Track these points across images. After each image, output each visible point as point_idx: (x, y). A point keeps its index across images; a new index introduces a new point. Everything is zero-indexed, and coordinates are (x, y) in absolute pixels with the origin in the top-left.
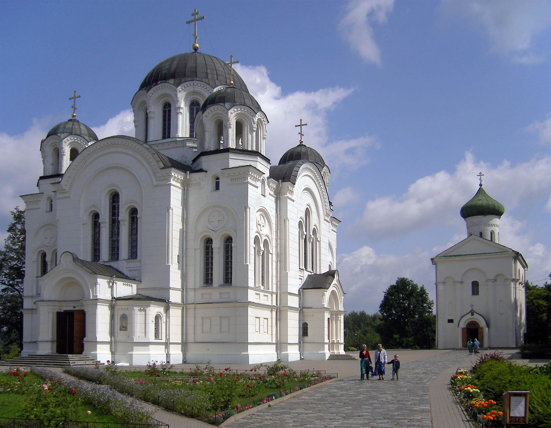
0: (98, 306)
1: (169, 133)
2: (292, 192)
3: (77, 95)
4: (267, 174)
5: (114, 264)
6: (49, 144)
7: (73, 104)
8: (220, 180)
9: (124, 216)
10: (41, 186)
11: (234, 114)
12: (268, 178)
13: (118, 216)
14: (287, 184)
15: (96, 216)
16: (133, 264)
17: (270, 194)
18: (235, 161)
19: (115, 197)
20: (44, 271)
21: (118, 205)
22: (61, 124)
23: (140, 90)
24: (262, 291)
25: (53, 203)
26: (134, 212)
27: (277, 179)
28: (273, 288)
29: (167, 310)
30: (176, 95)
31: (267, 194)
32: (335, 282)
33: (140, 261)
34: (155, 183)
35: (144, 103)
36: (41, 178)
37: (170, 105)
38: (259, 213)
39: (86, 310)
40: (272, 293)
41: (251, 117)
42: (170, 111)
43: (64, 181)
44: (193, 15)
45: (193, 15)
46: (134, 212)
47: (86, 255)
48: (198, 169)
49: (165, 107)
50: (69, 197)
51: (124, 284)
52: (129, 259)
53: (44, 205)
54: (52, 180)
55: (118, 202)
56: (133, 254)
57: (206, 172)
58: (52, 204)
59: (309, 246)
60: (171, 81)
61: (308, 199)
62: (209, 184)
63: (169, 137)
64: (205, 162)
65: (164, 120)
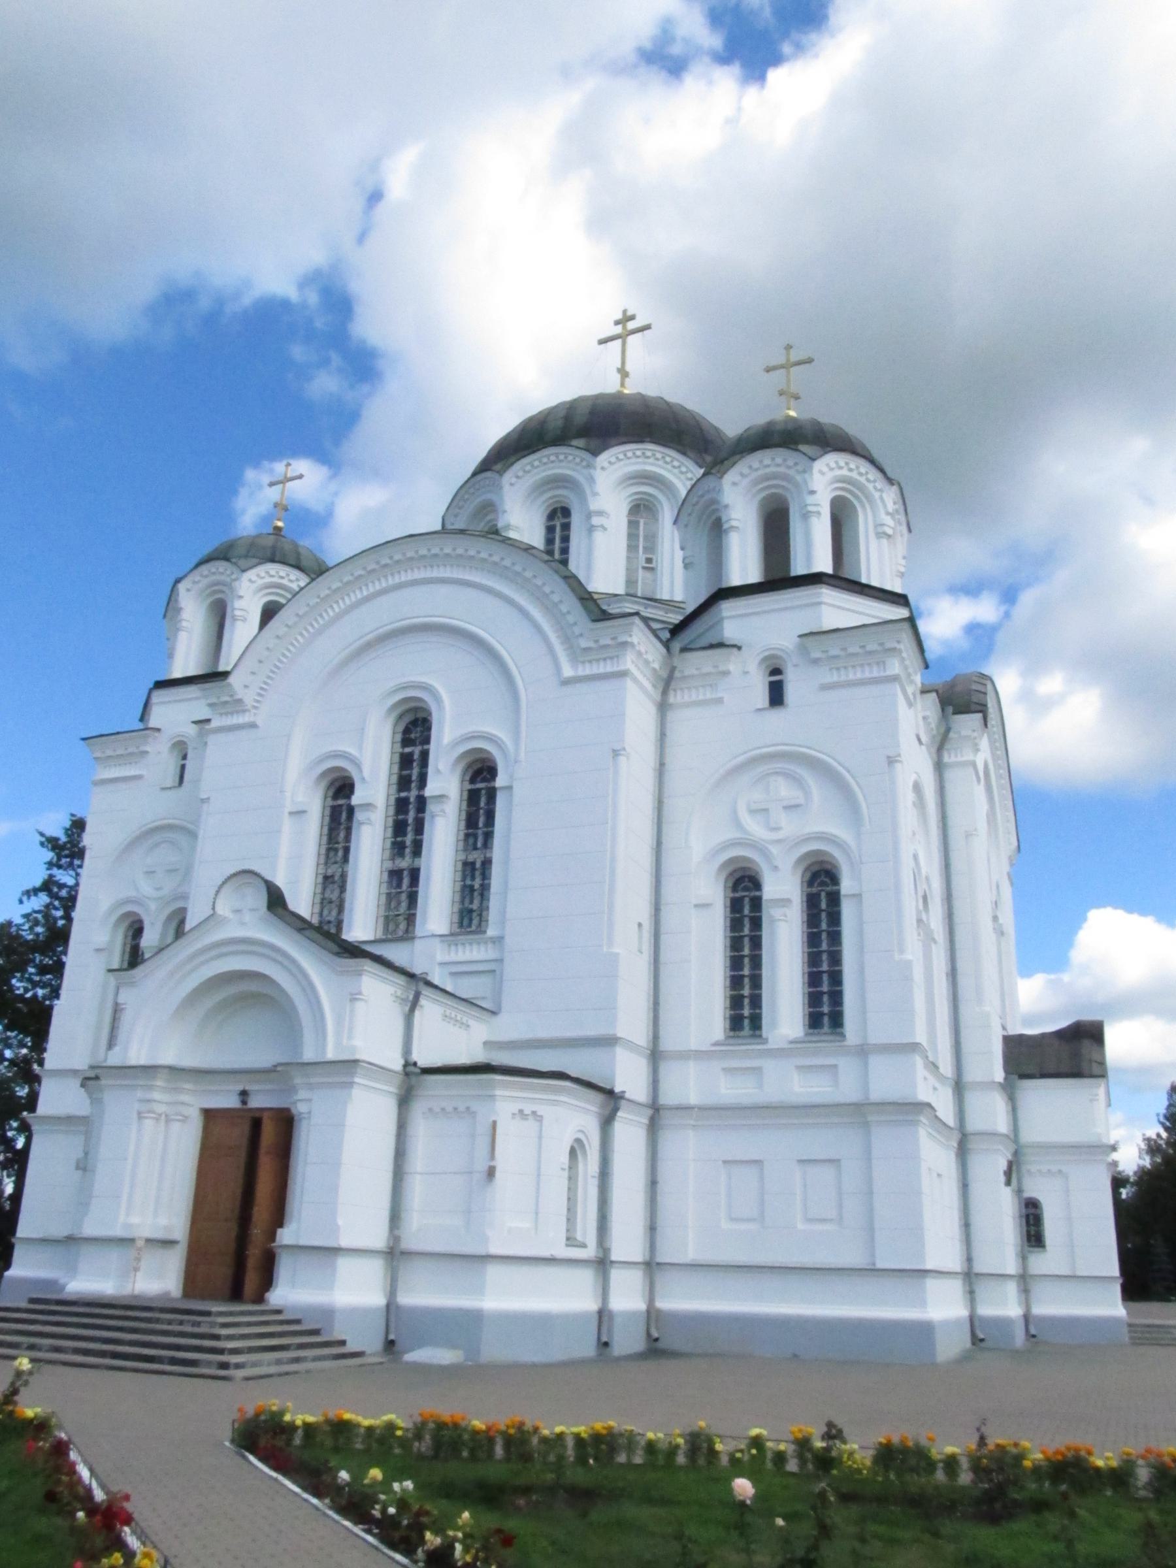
0: (356, 1092)
9: (445, 783)
11: (830, 475)
15: (341, 788)
16: (472, 952)
18: (837, 610)
25: (189, 764)
29: (607, 1122)
30: (591, 480)
33: (499, 940)
34: (568, 671)
37: (566, 512)
39: (300, 1108)
42: (566, 527)
44: (617, 323)
45: (617, 323)
46: (481, 773)
47: (302, 902)
48: (704, 642)
49: (552, 516)
50: (253, 726)
53: (159, 761)
55: (427, 740)
56: (471, 912)
58: (183, 767)
60: (580, 442)
64: (733, 620)
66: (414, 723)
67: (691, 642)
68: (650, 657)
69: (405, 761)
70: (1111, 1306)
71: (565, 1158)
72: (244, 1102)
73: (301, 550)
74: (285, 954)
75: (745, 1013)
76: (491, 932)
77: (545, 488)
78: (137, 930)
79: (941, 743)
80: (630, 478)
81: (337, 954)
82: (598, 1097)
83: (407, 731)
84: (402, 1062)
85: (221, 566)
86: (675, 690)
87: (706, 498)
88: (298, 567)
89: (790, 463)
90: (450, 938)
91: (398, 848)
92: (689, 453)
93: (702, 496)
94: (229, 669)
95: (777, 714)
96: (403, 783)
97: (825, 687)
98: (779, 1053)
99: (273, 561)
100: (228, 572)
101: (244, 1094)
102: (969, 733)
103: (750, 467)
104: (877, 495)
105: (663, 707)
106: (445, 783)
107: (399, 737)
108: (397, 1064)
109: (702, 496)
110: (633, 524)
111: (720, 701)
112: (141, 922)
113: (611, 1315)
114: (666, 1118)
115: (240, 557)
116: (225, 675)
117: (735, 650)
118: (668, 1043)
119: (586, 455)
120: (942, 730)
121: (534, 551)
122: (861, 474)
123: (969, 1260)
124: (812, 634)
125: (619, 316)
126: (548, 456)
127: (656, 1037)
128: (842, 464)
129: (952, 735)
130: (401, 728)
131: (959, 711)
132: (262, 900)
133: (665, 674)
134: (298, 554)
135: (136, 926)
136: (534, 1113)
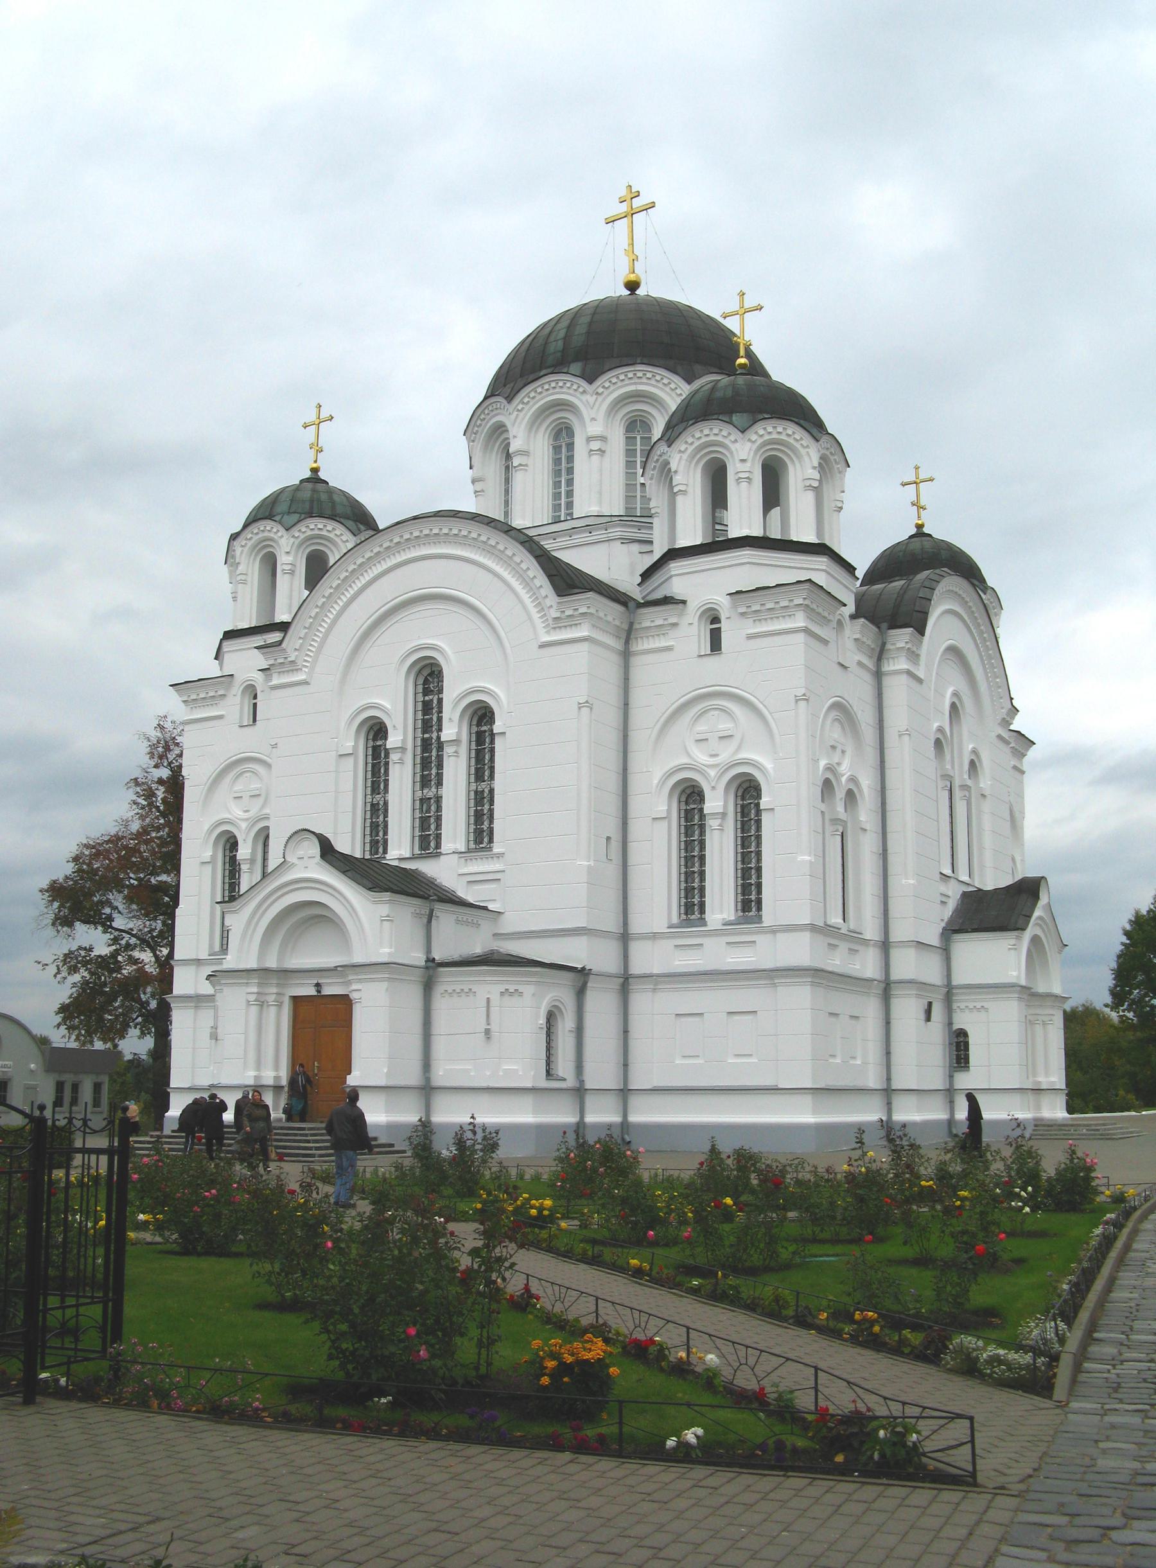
1: (570, 505)
2: (918, 656)
3: (324, 414)
4: (851, 608)
5: (428, 868)
6: (250, 543)
7: (313, 440)
8: (724, 625)
9: (453, 728)
10: (227, 657)
12: (853, 617)
13: (440, 730)
15: (376, 730)
17: (860, 664)
19: (428, 676)
21: (440, 701)
22: (283, 490)
23: (486, 398)
27: (874, 619)
29: (581, 992)
31: (853, 666)
32: (1037, 913)
35: (500, 429)
36: (229, 635)
37: (570, 432)
38: (834, 714)
39: (353, 996)
42: (570, 446)
43: (292, 641)
48: (658, 595)
49: (557, 435)
51: (458, 921)
52: (469, 851)
54: (259, 640)
55: (441, 691)
56: (482, 832)
57: (684, 602)
58: (255, 705)
60: (576, 367)
61: (953, 684)
62: (689, 634)
65: (557, 473)
66: (431, 674)
68: (610, 618)
70: (1056, 1110)
71: (542, 1021)
72: (319, 991)
74: (335, 889)
75: (692, 903)
76: (497, 849)
78: (231, 844)
80: (616, 404)
81: (370, 889)
82: (570, 975)
83: (426, 681)
84: (424, 958)
85: (268, 525)
88: (332, 517)
89: (724, 433)
90: (467, 854)
91: (425, 782)
92: (679, 369)
94: (285, 618)
95: (714, 662)
96: (426, 726)
97: (750, 637)
98: (715, 933)
99: (311, 515)
101: (318, 985)
103: (686, 442)
104: (803, 451)
105: (626, 655)
106: (453, 728)
107: (420, 689)
110: (630, 440)
112: (235, 837)
113: (584, 1123)
114: (634, 985)
115: (283, 514)
117: (681, 606)
118: (635, 927)
120: (880, 643)
123: (889, 1079)
127: (625, 923)
130: (420, 681)
131: (894, 626)
132: (315, 849)
133: (625, 626)
134: (333, 503)
135: (232, 841)
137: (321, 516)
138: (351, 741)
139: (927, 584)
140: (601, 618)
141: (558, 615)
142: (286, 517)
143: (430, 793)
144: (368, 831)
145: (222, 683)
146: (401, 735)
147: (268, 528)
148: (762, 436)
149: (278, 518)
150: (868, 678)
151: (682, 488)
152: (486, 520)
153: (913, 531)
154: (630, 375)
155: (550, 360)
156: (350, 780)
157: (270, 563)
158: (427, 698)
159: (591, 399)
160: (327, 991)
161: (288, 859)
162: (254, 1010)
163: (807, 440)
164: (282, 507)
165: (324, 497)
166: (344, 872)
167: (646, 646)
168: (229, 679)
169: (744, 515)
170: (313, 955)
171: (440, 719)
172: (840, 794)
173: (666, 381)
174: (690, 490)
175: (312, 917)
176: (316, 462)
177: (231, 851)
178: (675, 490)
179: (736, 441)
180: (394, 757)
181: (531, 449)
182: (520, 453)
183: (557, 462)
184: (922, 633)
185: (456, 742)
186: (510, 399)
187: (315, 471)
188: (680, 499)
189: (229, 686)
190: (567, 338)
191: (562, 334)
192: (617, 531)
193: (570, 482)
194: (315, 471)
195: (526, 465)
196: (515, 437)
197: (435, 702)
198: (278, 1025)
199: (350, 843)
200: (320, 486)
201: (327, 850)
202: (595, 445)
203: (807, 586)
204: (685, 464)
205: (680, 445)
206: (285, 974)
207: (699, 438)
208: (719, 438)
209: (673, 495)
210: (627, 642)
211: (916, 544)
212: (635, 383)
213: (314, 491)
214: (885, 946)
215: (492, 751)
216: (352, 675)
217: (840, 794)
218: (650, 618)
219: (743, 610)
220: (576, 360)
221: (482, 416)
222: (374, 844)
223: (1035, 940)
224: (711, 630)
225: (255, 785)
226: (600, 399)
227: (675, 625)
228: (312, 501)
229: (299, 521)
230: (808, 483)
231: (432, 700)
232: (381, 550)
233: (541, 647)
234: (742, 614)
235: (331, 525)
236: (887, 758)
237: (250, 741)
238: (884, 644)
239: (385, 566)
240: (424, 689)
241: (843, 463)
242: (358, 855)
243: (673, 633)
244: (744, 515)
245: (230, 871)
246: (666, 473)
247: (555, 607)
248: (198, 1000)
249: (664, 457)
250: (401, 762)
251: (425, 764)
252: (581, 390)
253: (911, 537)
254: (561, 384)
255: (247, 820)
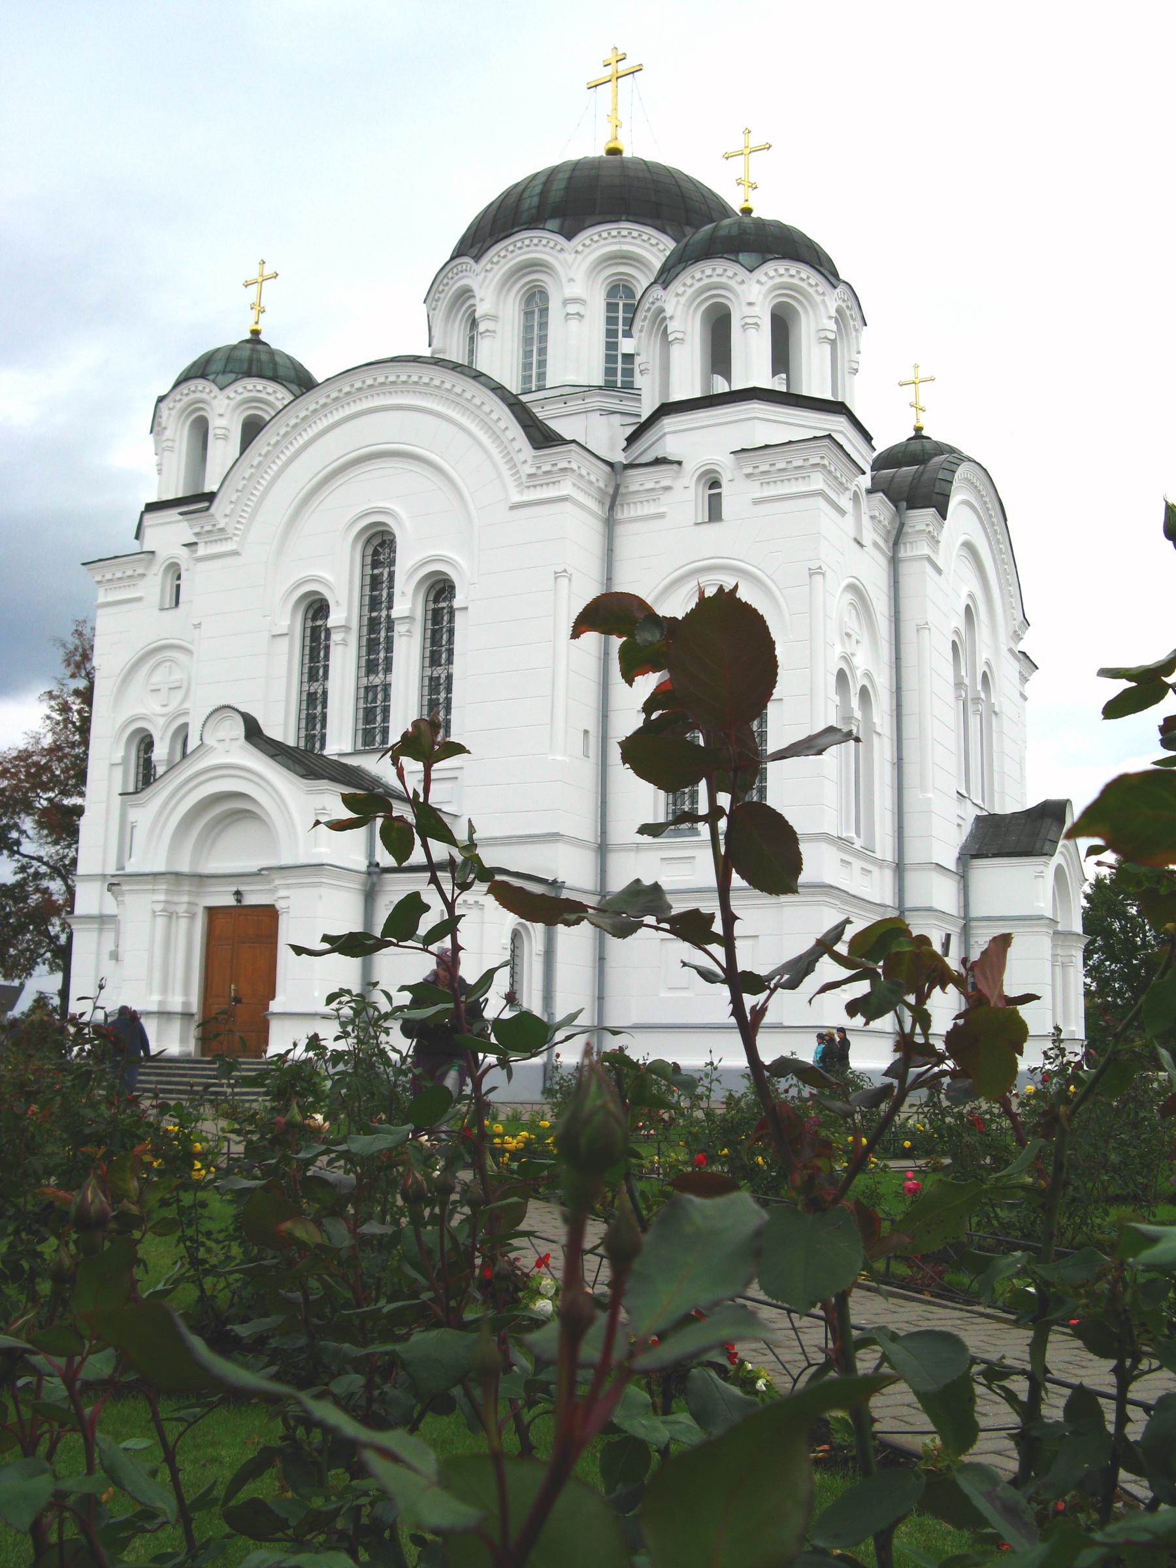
1: (542, 376)
2: (938, 542)
3: (268, 271)
6: (179, 406)
7: (254, 299)
8: (726, 490)
9: (407, 602)
10: (148, 533)
12: (869, 492)
13: (390, 607)
14: (922, 518)
17: (876, 544)
19: (379, 546)
20: (147, 776)
21: (391, 575)
23: (452, 258)
24: (857, 854)
25: (183, 583)
26: (440, 590)
28: (885, 849)
34: (517, 498)
35: (465, 294)
36: (151, 507)
39: (279, 905)
40: (880, 863)
41: (818, 299)
42: (544, 311)
47: (282, 726)
48: (649, 457)
50: (235, 553)
55: (392, 563)
57: (679, 463)
58: (178, 587)
59: (974, 722)
60: (553, 224)
62: (685, 496)
63: (541, 388)
65: (527, 341)
66: (382, 544)
67: (635, 459)
68: (593, 478)
69: (375, 582)
71: (507, 941)
72: (239, 901)
73: (278, 359)
77: (506, 287)
78: (146, 743)
79: (897, 538)
81: (303, 776)
83: (376, 553)
84: (366, 863)
85: (200, 384)
86: (622, 505)
87: (653, 308)
88: (274, 378)
91: (371, 667)
92: (668, 229)
93: (653, 303)
94: (215, 488)
96: (374, 604)
97: (757, 502)
99: (249, 374)
100: (207, 390)
102: (923, 527)
104: (818, 299)
105: (610, 524)
106: (407, 602)
107: (369, 560)
108: (362, 864)
109: (653, 303)
110: (611, 307)
111: (661, 516)
112: (151, 736)
116: (211, 497)
117: (675, 467)
119: (561, 240)
121: (482, 379)
122: (802, 279)
124: (743, 450)
125: (610, 56)
126: (522, 240)
127: (604, 832)
128: (781, 271)
129: (906, 529)
130: (370, 551)
131: (912, 506)
132: (238, 729)
133: (611, 491)
134: (275, 364)
135: (148, 740)
136: (476, 902)
137: (260, 376)
138: (288, 620)
139: (945, 465)
140: (581, 476)
141: (533, 471)
142: (220, 376)
143: (377, 680)
144: (303, 724)
145: (141, 560)
146: (344, 613)
147: (201, 388)
148: (771, 278)
149: (211, 377)
150: (883, 562)
151: (680, 336)
152: (451, 365)
153: (912, 434)
154: (614, 233)
155: (525, 217)
156: (286, 661)
157: (201, 428)
158: (376, 572)
159: (570, 257)
160: (249, 900)
161: (207, 741)
162: (161, 922)
163: (823, 286)
164: (216, 366)
165: (264, 357)
166: (273, 757)
167: (633, 514)
168: (150, 556)
169: (752, 364)
170: (233, 855)
171: (390, 597)
172: (854, 691)
173: (653, 241)
174: (688, 338)
175: (230, 811)
176: (257, 323)
177: (146, 752)
178: (671, 338)
179: (743, 282)
180: (336, 637)
181: (500, 314)
182: (486, 317)
183: (528, 328)
184: (944, 518)
185: (409, 619)
186: (477, 258)
187: (256, 333)
188: (675, 350)
189: (151, 562)
190: (543, 194)
191: (538, 190)
192: (596, 401)
193: (543, 351)
194: (256, 333)
195: (494, 332)
196: (482, 300)
197: (386, 575)
198: (189, 941)
199: (282, 726)
200: (260, 347)
201: (253, 732)
202: (572, 309)
203: (827, 442)
204: (682, 309)
205: (677, 286)
206: (200, 879)
207: (700, 279)
208: (723, 280)
209: (666, 342)
210: (612, 508)
211: (916, 446)
212: (620, 243)
213: (253, 350)
214: (900, 868)
215: (451, 632)
216: (289, 541)
217: (854, 691)
218: (639, 480)
219: (749, 470)
220: (553, 216)
221: (445, 281)
222: (310, 738)
223: (1059, 871)
224: (710, 496)
225: (177, 676)
226: (580, 257)
227: (667, 488)
228: (252, 360)
229: (236, 380)
230: (822, 334)
231: (382, 574)
232: (328, 401)
233: (512, 508)
234: (748, 476)
235: (271, 386)
236: (903, 655)
237: (168, 627)
238: (902, 525)
239: (331, 420)
240: (373, 561)
241: (859, 322)
242: (291, 742)
243: (666, 497)
244: (752, 364)
245: (144, 776)
246: (660, 320)
247: (530, 462)
248: (103, 920)
249: (657, 304)
250: (345, 643)
251: (372, 646)
252: (558, 247)
253: (909, 439)
254: (535, 241)
255: (162, 715)
